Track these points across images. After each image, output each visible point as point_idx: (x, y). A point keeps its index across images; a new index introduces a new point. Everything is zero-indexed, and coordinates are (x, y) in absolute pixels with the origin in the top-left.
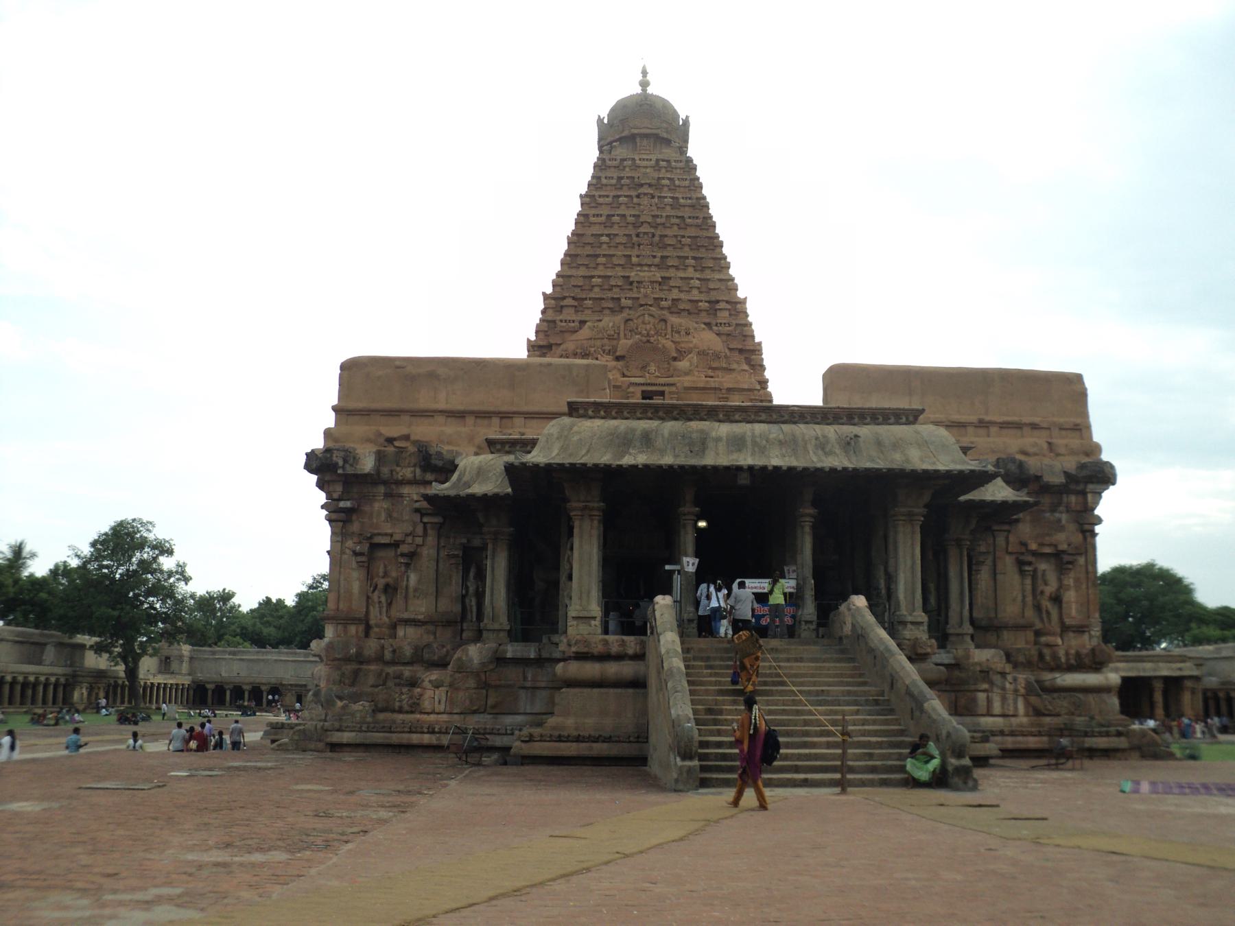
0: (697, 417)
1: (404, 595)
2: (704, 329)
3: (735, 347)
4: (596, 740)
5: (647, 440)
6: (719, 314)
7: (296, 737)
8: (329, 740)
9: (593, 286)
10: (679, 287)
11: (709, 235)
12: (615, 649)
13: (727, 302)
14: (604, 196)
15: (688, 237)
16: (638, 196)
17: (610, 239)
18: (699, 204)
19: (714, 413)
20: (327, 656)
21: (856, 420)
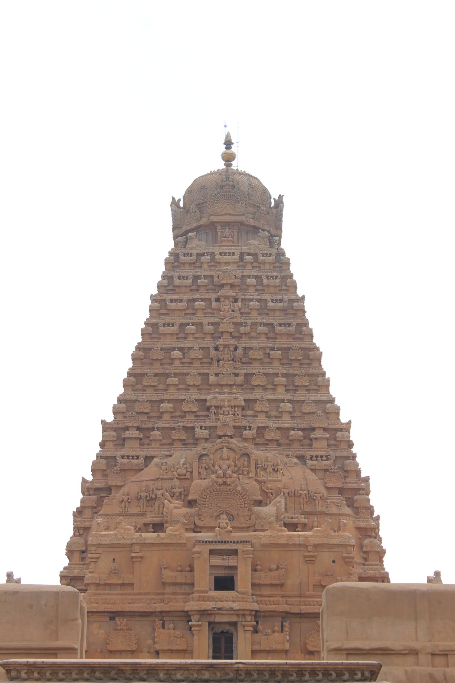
0: (137, 676)
2: (296, 464)
3: (334, 485)
6: (315, 444)
10: (267, 412)
13: (325, 429)
14: (176, 300)
15: (279, 349)
16: (217, 300)
17: (184, 354)
18: (292, 308)
19: (154, 672)
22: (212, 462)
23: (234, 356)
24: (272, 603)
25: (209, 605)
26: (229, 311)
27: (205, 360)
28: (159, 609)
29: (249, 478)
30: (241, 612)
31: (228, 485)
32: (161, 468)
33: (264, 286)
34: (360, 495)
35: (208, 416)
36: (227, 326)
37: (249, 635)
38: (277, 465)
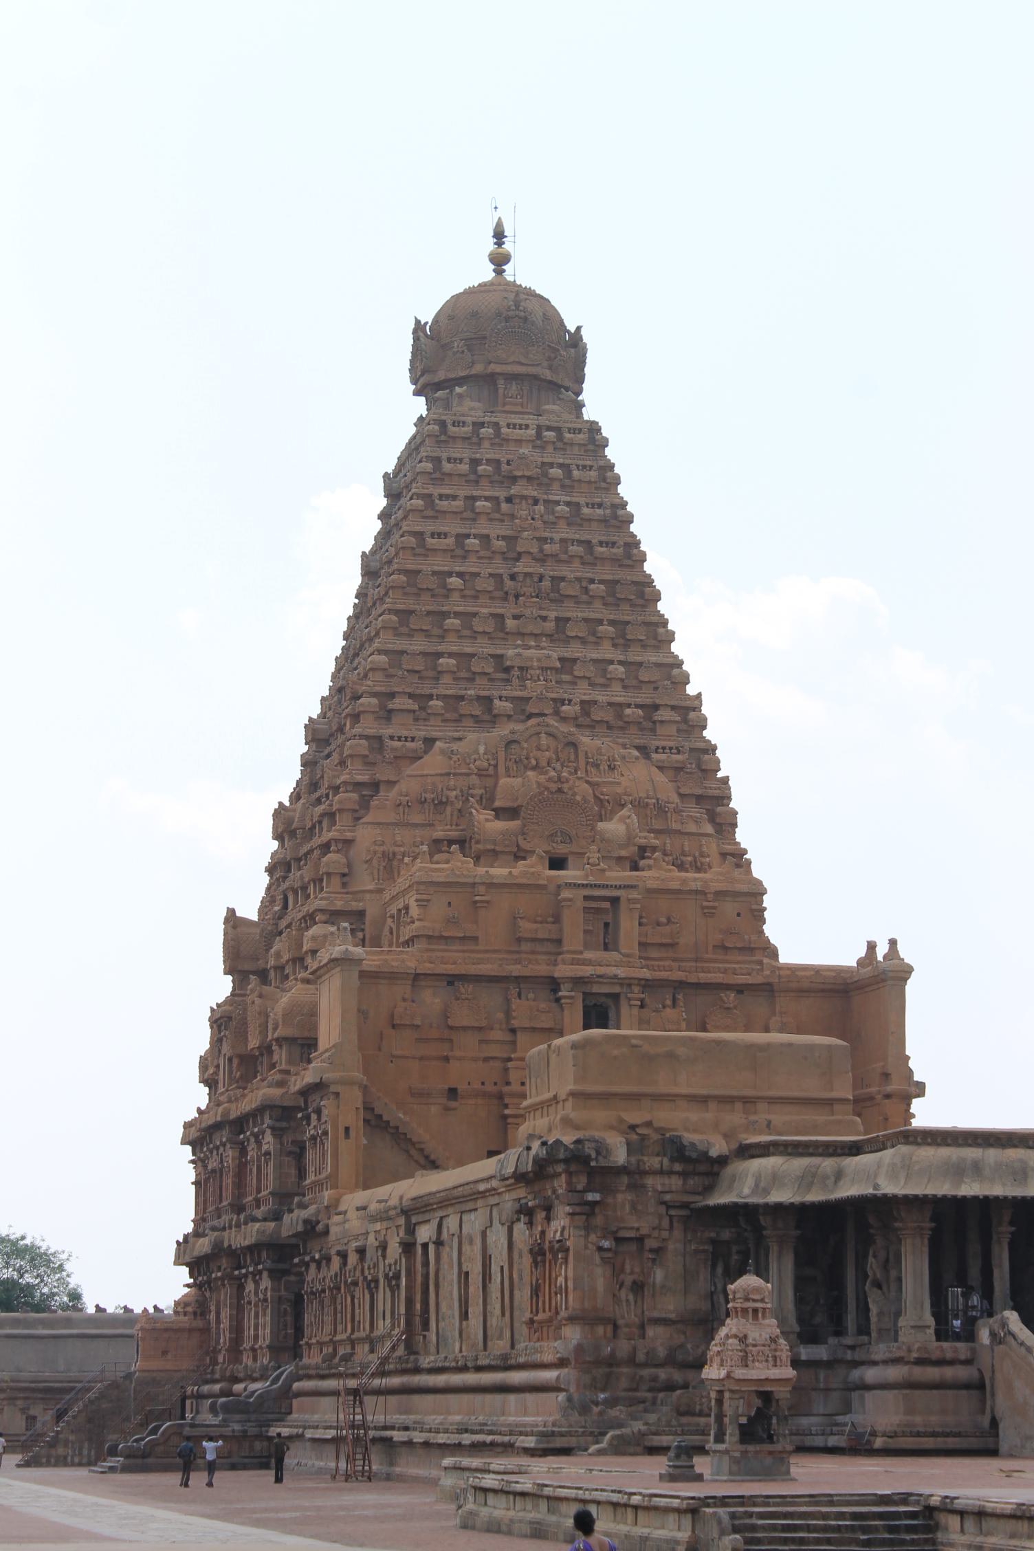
2: (637, 758)
4: (947, 1435)
5: (977, 1169)
6: (660, 730)
7: (615, 1443)
8: (648, 1444)
10: (589, 678)
11: (635, 579)
12: (949, 1355)
13: (673, 708)
14: (447, 497)
15: (601, 582)
16: (509, 500)
18: (615, 517)
20: (576, 1360)
23: (540, 590)
24: (662, 968)
25: (587, 971)
26: (527, 519)
28: (514, 974)
29: (579, 778)
30: (627, 981)
37: (635, 1011)
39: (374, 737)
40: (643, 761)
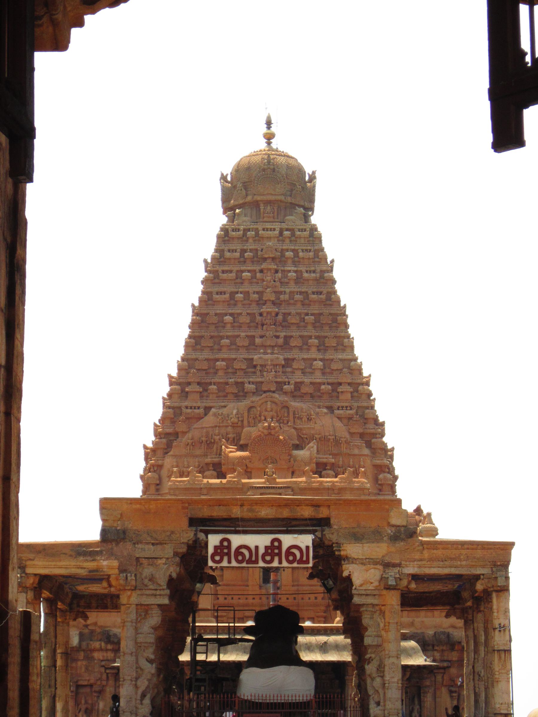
1: (96, 714)
2: (326, 413)
3: (356, 431)
6: (341, 397)
9: (217, 370)
10: (302, 369)
11: (332, 312)
13: (349, 384)
15: (312, 315)
16: (261, 271)
17: (234, 318)
18: (323, 278)
21: (329, 632)
22: (258, 413)
23: (276, 321)
27: (252, 324)
31: (272, 435)
32: (218, 418)
33: (300, 258)
34: (376, 438)
35: (255, 372)
36: (269, 295)
38: (311, 415)
39: (177, 407)
40: (329, 415)
